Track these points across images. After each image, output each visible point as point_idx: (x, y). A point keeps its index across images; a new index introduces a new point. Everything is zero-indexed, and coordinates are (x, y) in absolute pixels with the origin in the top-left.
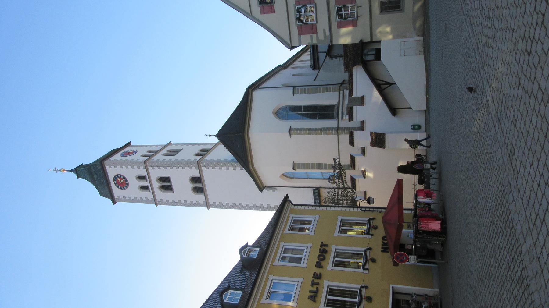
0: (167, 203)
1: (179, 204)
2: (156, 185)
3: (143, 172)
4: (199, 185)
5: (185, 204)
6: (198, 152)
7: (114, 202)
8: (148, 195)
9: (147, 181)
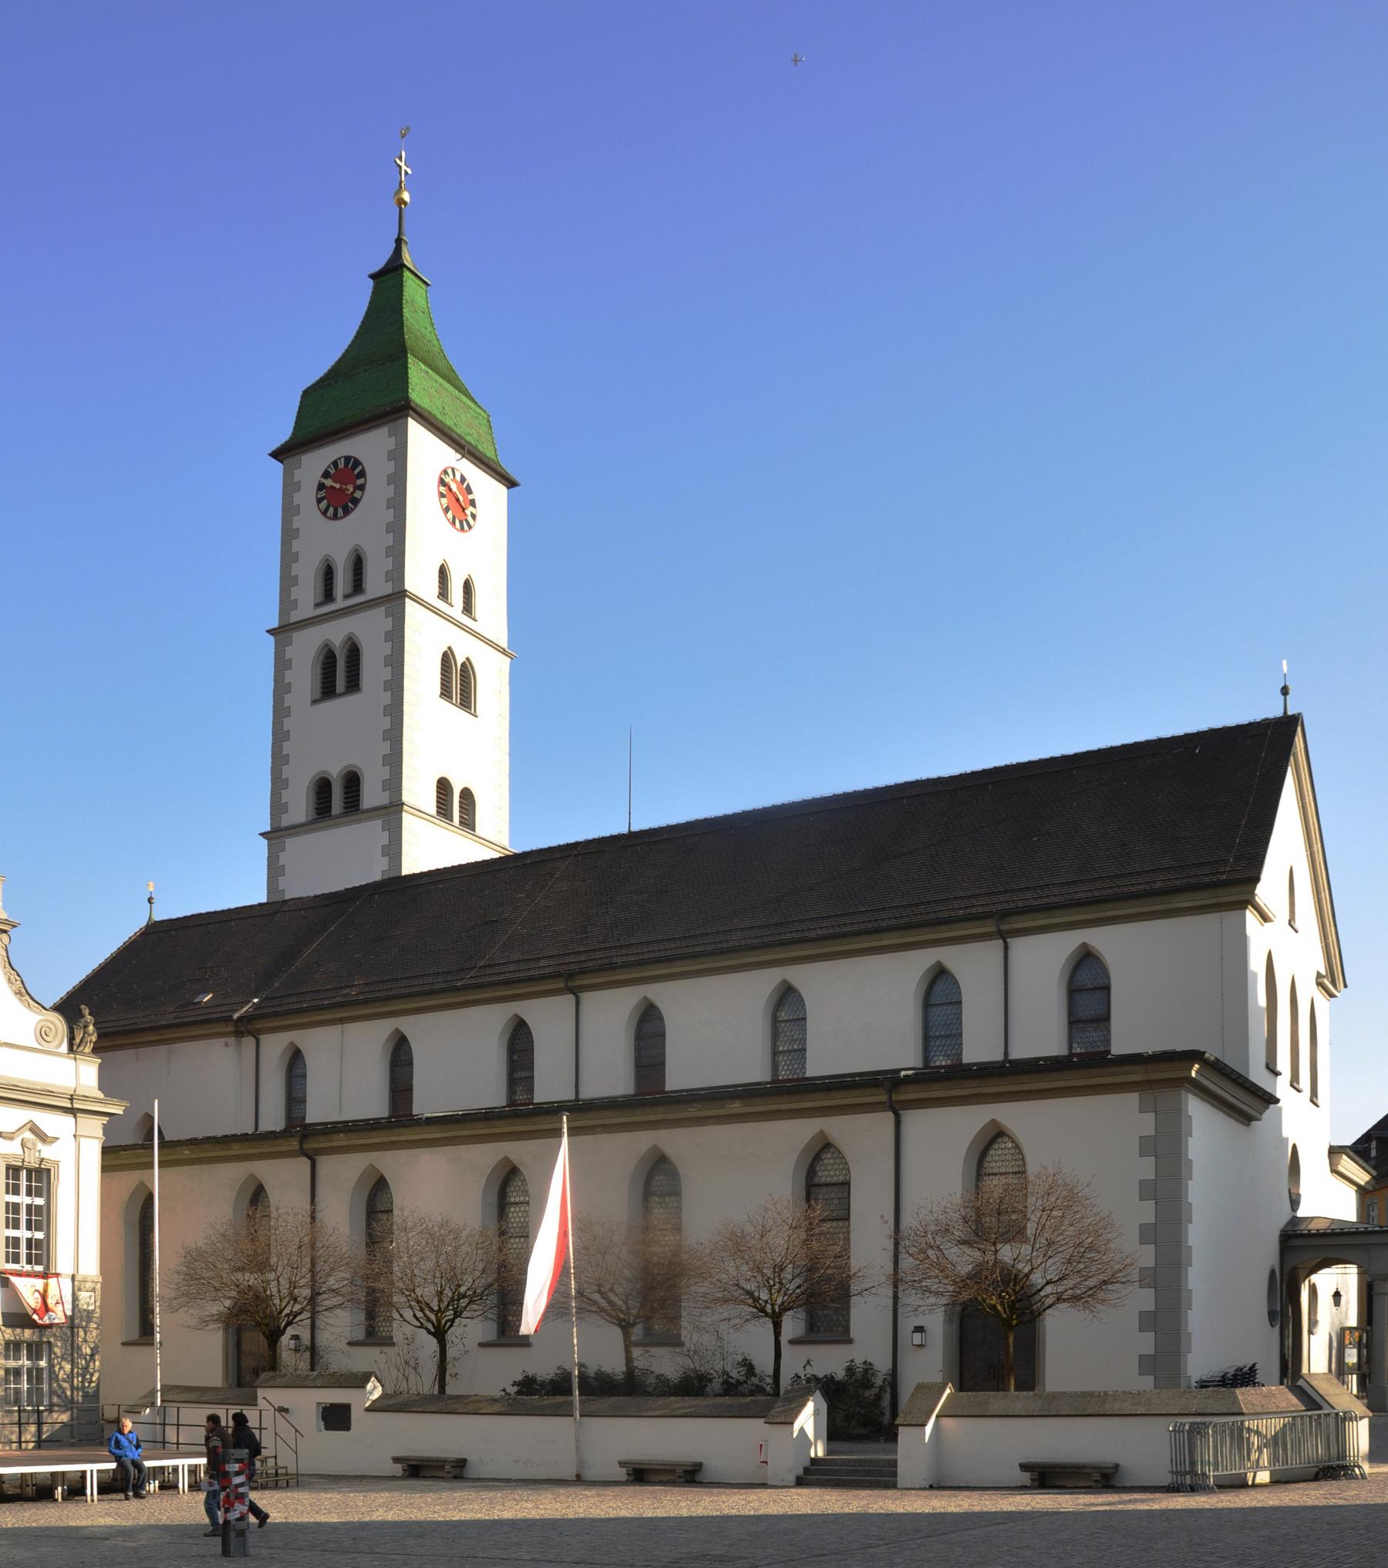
0: (281, 688)
1: (280, 735)
2: (335, 633)
3: (376, 585)
5: (279, 759)
7: (278, 454)
8: (307, 592)
9: (346, 597)
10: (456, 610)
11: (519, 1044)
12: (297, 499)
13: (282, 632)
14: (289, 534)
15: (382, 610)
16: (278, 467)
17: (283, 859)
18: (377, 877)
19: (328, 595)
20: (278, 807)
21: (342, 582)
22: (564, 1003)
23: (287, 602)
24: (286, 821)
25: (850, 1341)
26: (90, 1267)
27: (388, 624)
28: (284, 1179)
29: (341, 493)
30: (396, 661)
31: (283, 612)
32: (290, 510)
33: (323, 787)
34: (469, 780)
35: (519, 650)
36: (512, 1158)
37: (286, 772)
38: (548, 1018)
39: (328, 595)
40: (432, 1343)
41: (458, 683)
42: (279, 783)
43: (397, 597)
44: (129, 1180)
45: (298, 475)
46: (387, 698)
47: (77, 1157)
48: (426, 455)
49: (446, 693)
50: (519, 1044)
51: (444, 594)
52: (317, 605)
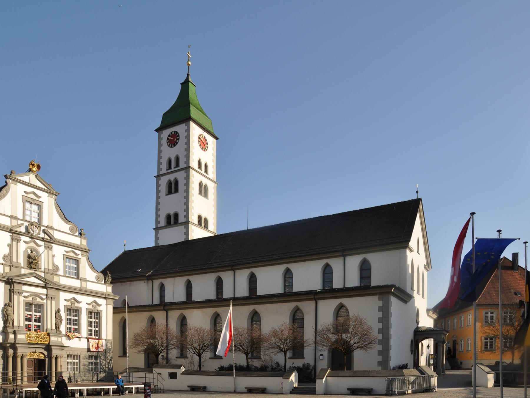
0: (158, 191)
1: (158, 204)
2: (172, 177)
3: (182, 165)
5: (157, 210)
8: (164, 167)
9: (174, 168)
10: (203, 172)
11: (219, 283)
12: (162, 142)
13: (158, 177)
14: (160, 151)
15: (183, 171)
16: (157, 134)
17: (159, 235)
18: (183, 240)
20: (157, 222)
22: (231, 273)
23: (159, 169)
24: (159, 226)
25: (304, 358)
26: (110, 337)
27: (185, 175)
28: (160, 317)
29: (173, 141)
30: (187, 185)
31: (158, 172)
32: (160, 145)
33: (168, 217)
34: (205, 215)
35: (219, 181)
36: (218, 312)
37: (159, 213)
38: (227, 277)
39: (170, 167)
40: (198, 358)
41: (203, 190)
42: (157, 216)
43: (187, 168)
44: (120, 316)
45: (162, 136)
46: (185, 194)
47: (106, 309)
48: (195, 131)
49: (200, 193)
50: (219, 283)
51: (200, 167)
52: (167, 170)
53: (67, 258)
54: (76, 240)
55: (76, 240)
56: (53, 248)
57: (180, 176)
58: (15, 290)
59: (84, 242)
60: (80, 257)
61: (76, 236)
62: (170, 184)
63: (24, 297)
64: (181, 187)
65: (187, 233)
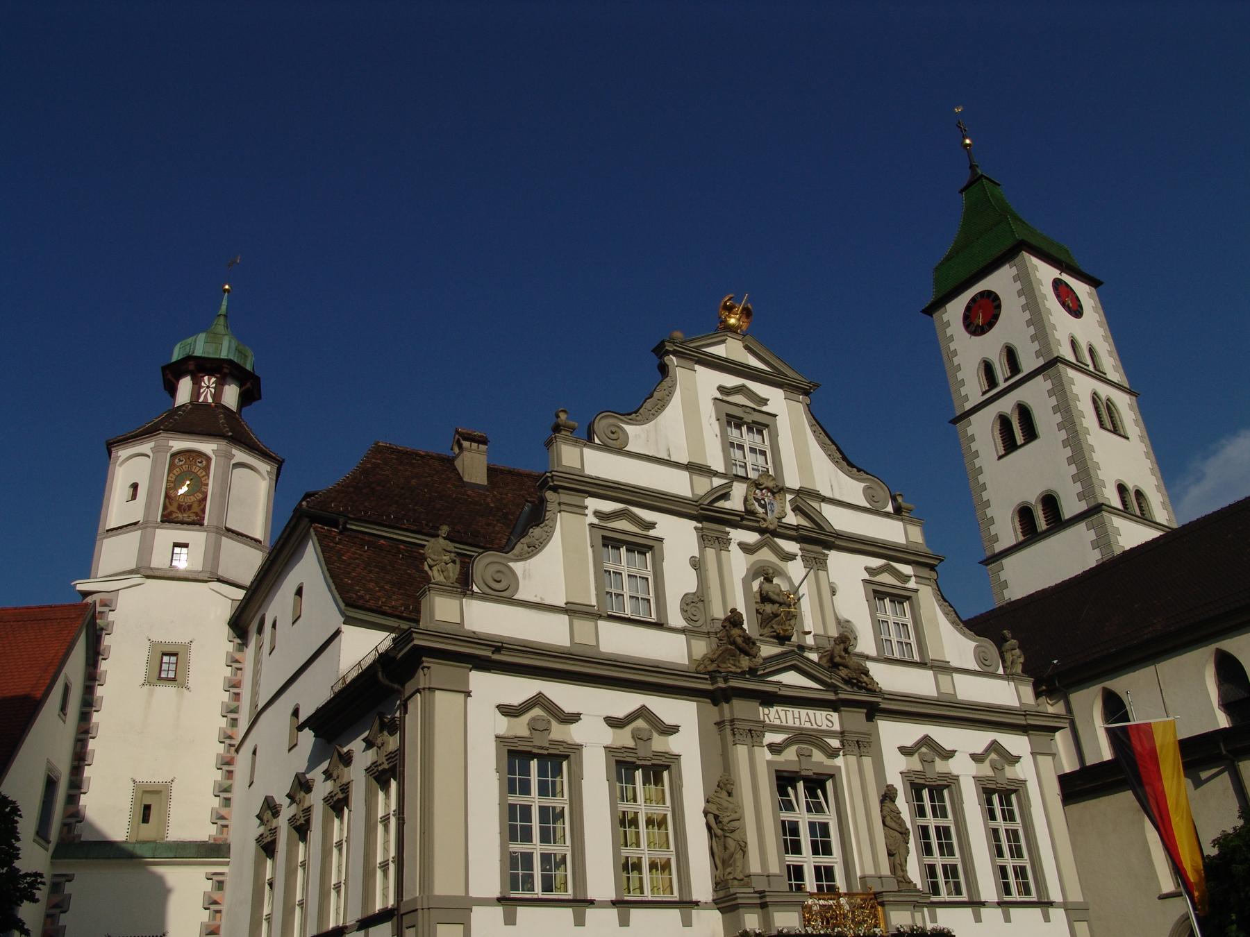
2: (1006, 405)
3: (1028, 363)
4: (1042, 524)
6: (1130, 486)
9: (1006, 380)
19: (992, 382)
21: (1001, 371)
33: (1025, 514)
39: (992, 382)
52: (984, 393)
53: (878, 594)
54: (892, 531)
55: (892, 531)
56: (830, 558)
57: (1036, 394)
58: (737, 724)
59: (916, 535)
60: (912, 584)
61: (887, 515)
62: (1004, 421)
63: (775, 749)
64: (1045, 419)
65: (1103, 539)
